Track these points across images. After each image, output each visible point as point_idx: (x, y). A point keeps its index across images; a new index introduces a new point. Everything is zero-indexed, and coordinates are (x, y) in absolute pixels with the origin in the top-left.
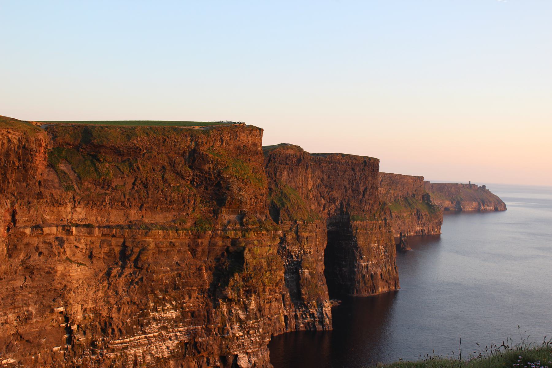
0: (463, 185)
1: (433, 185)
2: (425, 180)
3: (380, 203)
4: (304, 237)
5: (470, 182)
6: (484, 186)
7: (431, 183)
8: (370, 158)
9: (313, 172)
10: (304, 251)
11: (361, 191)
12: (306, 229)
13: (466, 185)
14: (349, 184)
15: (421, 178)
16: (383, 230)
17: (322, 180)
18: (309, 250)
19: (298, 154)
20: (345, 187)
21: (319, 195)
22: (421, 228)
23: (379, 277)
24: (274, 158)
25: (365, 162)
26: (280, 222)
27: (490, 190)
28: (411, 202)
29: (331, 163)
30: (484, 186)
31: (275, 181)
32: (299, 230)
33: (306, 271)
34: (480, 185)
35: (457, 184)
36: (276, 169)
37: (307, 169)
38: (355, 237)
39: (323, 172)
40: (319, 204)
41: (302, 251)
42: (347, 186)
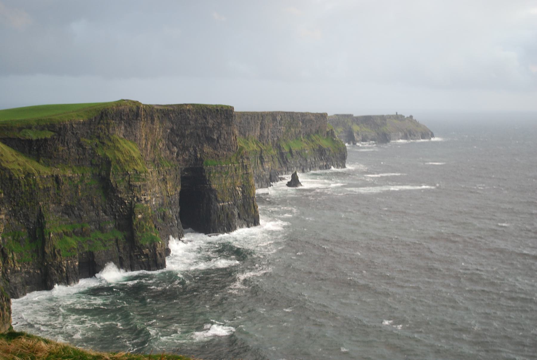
0: (390, 117)
1: (357, 118)
3: (237, 147)
4: (136, 186)
5: (397, 113)
6: (411, 117)
7: (355, 115)
8: (222, 107)
9: (161, 122)
10: (137, 199)
11: (215, 137)
12: (138, 179)
13: (393, 116)
14: (202, 131)
15: (323, 116)
16: (240, 172)
17: (172, 130)
18: (143, 197)
19: (135, 108)
20: (198, 135)
21: (171, 144)
22: (325, 164)
23: (237, 216)
24: (106, 115)
25: (217, 110)
26: (111, 173)
28: (314, 138)
29: (181, 113)
30: (411, 117)
31: (108, 136)
32: (131, 180)
33: (140, 216)
34: (406, 115)
35: (383, 116)
36: (108, 124)
37: (152, 120)
38: (209, 180)
39: (172, 123)
40: (172, 153)
41: (135, 199)
42: (200, 134)
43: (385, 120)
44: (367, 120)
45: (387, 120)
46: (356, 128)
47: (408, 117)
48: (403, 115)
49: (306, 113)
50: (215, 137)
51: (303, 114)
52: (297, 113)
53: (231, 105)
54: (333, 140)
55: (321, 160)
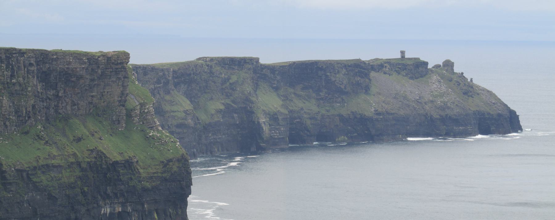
0: (379, 66)
1: (272, 68)
2: (134, 61)
5: (403, 53)
6: (449, 65)
13: (389, 62)
30: (449, 65)
34: (433, 59)
43: (367, 75)
44: (306, 75)
45: (373, 74)
46: (268, 102)
47: (438, 66)
48: (423, 59)
49: (56, 53)
51: (43, 57)
52: (21, 52)
54: (147, 138)
55: (106, 197)
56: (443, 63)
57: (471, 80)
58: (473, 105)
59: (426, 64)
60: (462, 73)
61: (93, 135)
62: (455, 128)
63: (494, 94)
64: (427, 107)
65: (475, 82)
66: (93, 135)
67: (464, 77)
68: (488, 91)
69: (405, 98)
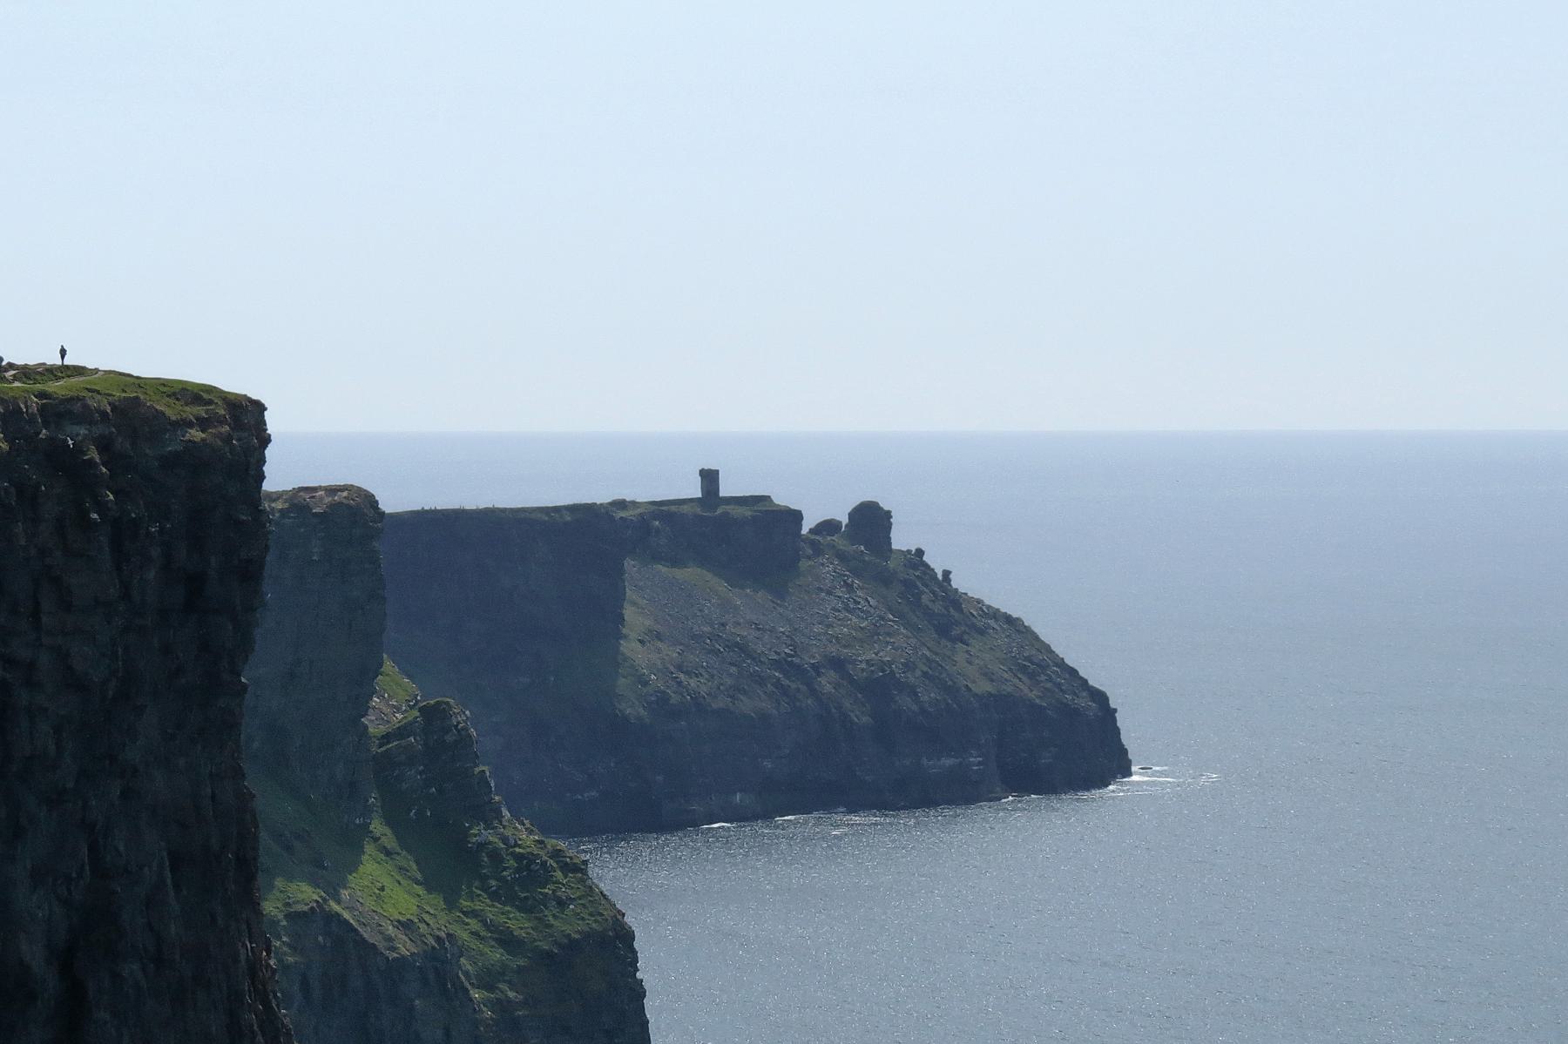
5: (710, 478)
6: (871, 521)
13: (665, 513)
27: (936, 562)
30: (871, 521)
47: (829, 527)
48: (782, 498)
50: (33, 952)
53: (230, 376)
56: (851, 515)
57: (947, 574)
58: (976, 669)
59: (796, 516)
60: (920, 552)
61: (289, 849)
62: (925, 761)
63: (1028, 630)
64: (827, 683)
65: (957, 582)
66: (289, 849)
67: (927, 566)
68: (1010, 620)
69: (742, 648)
